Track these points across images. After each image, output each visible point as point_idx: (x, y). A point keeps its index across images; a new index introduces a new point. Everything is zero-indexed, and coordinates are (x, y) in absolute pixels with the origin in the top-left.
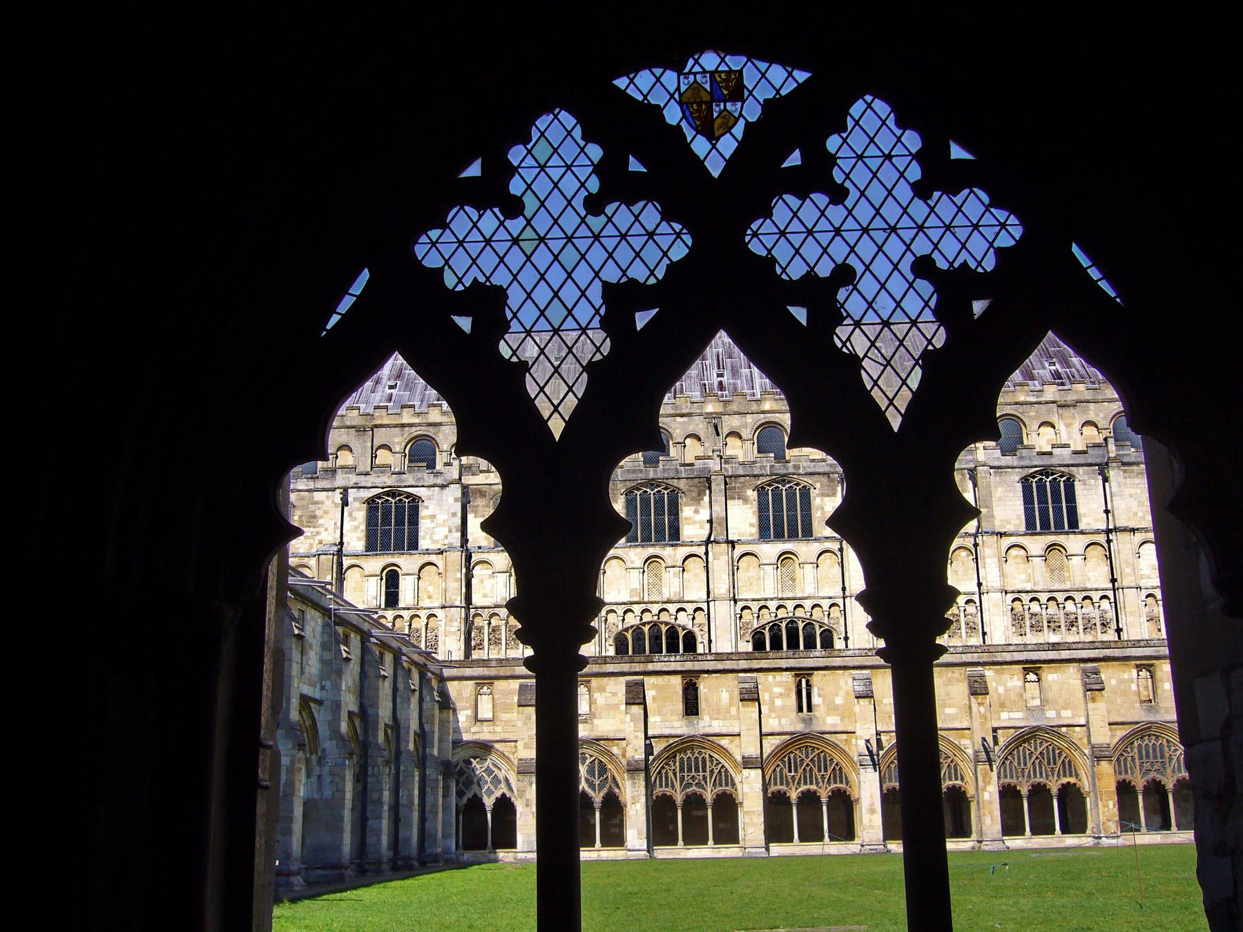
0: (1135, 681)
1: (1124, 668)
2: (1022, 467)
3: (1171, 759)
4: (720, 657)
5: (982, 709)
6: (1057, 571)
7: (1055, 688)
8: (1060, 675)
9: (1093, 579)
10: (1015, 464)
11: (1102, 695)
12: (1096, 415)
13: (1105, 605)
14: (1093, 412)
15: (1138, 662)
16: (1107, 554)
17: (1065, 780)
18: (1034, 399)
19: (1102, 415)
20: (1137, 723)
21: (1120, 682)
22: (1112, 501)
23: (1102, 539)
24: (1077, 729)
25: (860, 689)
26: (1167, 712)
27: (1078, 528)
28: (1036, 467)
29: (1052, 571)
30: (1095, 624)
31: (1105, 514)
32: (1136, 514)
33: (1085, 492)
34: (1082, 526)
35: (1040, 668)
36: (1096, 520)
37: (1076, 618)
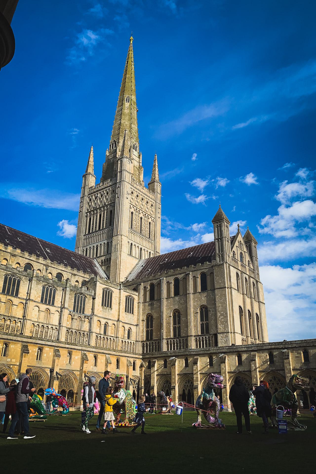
1: (35, 347)
6: (9, 309)
7: (12, 350)
8: (15, 346)
9: (17, 314)
11: (28, 355)
13: (19, 324)
14: (20, 260)
15: (39, 346)
16: (24, 307)
18: (4, 250)
21: (32, 351)
22: (30, 290)
23: (24, 302)
24: (16, 367)
26: (43, 364)
27: (18, 296)
28: (11, 272)
29: (6, 309)
30: (14, 330)
31: (27, 294)
32: (35, 296)
33: (23, 285)
34: (19, 296)
36: (24, 295)
37: (9, 327)
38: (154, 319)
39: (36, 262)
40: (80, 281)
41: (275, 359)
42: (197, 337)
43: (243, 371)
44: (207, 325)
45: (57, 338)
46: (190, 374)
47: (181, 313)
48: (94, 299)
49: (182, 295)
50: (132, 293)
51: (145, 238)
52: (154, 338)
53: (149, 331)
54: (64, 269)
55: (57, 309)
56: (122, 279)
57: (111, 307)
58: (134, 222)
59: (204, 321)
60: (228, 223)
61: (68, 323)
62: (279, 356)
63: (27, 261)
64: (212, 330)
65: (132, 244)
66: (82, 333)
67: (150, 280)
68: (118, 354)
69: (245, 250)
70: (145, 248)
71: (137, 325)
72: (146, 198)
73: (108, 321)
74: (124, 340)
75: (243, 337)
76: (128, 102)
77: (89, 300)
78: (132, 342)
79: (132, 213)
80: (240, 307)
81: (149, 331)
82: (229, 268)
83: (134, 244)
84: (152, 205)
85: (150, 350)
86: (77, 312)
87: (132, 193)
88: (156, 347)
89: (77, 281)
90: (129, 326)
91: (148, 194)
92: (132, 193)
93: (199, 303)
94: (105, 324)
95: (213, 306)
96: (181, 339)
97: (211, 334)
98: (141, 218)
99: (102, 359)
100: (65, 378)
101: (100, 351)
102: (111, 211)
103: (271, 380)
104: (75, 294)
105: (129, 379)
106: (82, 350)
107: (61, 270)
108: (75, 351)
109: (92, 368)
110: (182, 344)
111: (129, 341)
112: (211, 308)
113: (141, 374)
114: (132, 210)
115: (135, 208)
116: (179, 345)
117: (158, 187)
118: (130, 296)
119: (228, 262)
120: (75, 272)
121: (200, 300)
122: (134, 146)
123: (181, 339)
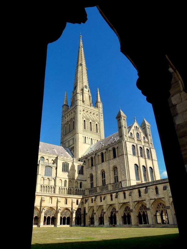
41: (141, 194)
43: (127, 203)
47: (105, 172)
48: (56, 168)
52: (94, 187)
54: (44, 155)
56: (80, 157)
58: (86, 125)
61: (41, 182)
65: (85, 137)
66: (50, 186)
69: (140, 130)
71: (86, 180)
74: (77, 189)
75: (138, 182)
78: (83, 190)
79: (85, 121)
82: (126, 143)
83: (86, 137)
84: (97, 115)
87: (84, 110)
89: (53, 160)
90: (81, 181)
91: (94, 109)
92: (84, 110)
96: (106, 186)
98: (91, 123)
99: (54, 200)
101: (53, 196)
102: (74, 122)
103: (141, 207)
109: (49, 205)
111: (81, 189)
114: (84, 119)
115: (86, 118)
117: (100, 105)
119: (125, 139)
120: (51, 156)
122: (85, 86)
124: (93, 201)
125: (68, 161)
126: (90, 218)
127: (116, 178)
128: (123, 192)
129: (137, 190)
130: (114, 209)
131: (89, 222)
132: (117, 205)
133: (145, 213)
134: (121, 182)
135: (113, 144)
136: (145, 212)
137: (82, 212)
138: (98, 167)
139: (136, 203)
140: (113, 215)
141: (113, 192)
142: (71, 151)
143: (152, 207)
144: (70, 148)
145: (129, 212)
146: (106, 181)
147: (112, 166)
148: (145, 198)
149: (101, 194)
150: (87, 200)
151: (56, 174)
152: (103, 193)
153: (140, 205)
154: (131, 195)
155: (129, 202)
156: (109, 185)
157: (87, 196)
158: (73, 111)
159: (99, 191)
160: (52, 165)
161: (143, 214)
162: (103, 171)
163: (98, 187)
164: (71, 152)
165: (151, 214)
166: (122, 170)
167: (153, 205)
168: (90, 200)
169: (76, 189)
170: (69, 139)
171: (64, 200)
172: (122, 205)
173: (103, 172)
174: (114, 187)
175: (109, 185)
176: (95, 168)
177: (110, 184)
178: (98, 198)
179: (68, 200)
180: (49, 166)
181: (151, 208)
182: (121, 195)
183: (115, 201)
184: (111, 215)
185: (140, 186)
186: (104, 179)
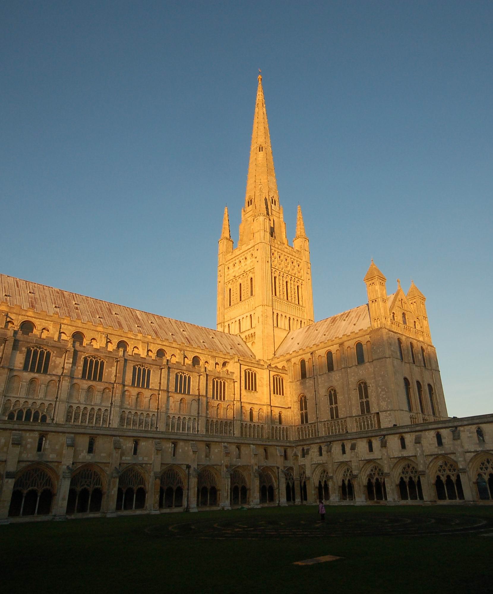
0: (171, 448)
2: (135, 361)
3: (176, 478)
4: (58, 425)
5: (117, 455)
10: (133, 359)
12: (153, 348)
17: (140, 486)
18: (134, 337)
19: (155, 349)
20: (169, 464)
25: (69, 442)
28: (140, 362)
30: (149, 425)
35: (139, 440)
38: (308, 399)
39: (170, 347)
40: (220, 363)
41: (443, 441)
42: (357, 418)
43: (408, 457)
44: (368, 403)
45: (196, 430)
46: (348, 461)
49: (337, 370)
50: (282, 372)
51: (294, 305)
52: (309, 422)
53: (304, 414)
54: (201, 352)
55: (193, 398)
57: (255, 390)
59: (363, 399)
60: (383, 280)
62: (448, 437)
63: (160, 347)
64: (373, 408)
67: (300, 355)
68: (265, 443)
70: (294, 317)
72: (291, 258)
73: (253, 406)
75: (412, 414)
76: (262, 151)
77: (229, 384)
80: (406, 379)
81: (304, 414)
85: (306, 435)
86: (217, 398)
88: (312, 431)
90: (280, 409)
93: (356, 378)
94: (251, 409)
95: (373, 381)
97: (373, 413)
100: (205, 473)
103: (441, 466)
104: (213, 380)
105: (280, 470)
106: (221, 442)
107: (198, 353)
108: (214, 443)
110: (341, 427)
112: (370, 383)
113: (294, 464)
116: (337, 428)
118: (278, 375)
121: (357, 374)
122: (272, 200)
123: (340, 421)
124: (324, 453)
125: (256, 366)
126: (316, 487)
127: (365, 407)
128: (398, 435)
129: (432, 433)
130: (376, 469)
131: (315, 494)
132: (386, 462)
133: (454, 479)
134: (378, 413)
135: (357, 333)
136: (451, 475)
137: (295, 474)
138: (320, 380)
139: (431, 459)
140: (374, 481)
141: (373, 434)
142: (245, 342)
143: (470, 466)
144: (243, 336)
145: (412, 475)
146: (339, 411)
147: (353, 380)
148: (452, 449)
149: (343, 438)
150: (308, 450)
151: (234, 394)
152: (349, 437)
153: (440, 463)
154: (419, 443)
155: (416, 456)
156: (348, 419)
157: (308, 442)
158: (250, 254)
159: (322, 433)
160: (226, 376)
161: (446, 481)
162: (332, 390)
163: (321, 422)
164: (247, 346)
165: (470, 480)
166: (380, 390)
167: (471, 464)
168: (314, 451)
169: (273, 427)
170: (241, 318)
171: (261, 451)
172: (397, 462)
173: (332, 392)
174: (360, 423)
175: (348, 419)
176: (312, 382)
177: (350, 417)
178: (336, 448)
179: (271, 450)
180: (219, 378)
181: (468, 469)
182: (394, 442)
183: (377, 453)
184: (369, 482)
185: (440, 426)
186: (334, 406)
